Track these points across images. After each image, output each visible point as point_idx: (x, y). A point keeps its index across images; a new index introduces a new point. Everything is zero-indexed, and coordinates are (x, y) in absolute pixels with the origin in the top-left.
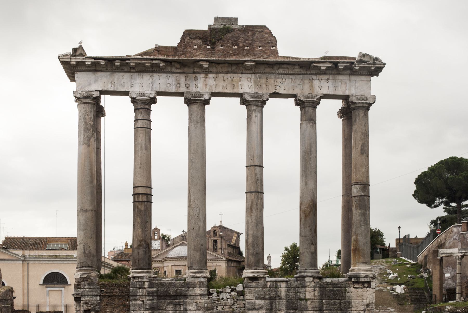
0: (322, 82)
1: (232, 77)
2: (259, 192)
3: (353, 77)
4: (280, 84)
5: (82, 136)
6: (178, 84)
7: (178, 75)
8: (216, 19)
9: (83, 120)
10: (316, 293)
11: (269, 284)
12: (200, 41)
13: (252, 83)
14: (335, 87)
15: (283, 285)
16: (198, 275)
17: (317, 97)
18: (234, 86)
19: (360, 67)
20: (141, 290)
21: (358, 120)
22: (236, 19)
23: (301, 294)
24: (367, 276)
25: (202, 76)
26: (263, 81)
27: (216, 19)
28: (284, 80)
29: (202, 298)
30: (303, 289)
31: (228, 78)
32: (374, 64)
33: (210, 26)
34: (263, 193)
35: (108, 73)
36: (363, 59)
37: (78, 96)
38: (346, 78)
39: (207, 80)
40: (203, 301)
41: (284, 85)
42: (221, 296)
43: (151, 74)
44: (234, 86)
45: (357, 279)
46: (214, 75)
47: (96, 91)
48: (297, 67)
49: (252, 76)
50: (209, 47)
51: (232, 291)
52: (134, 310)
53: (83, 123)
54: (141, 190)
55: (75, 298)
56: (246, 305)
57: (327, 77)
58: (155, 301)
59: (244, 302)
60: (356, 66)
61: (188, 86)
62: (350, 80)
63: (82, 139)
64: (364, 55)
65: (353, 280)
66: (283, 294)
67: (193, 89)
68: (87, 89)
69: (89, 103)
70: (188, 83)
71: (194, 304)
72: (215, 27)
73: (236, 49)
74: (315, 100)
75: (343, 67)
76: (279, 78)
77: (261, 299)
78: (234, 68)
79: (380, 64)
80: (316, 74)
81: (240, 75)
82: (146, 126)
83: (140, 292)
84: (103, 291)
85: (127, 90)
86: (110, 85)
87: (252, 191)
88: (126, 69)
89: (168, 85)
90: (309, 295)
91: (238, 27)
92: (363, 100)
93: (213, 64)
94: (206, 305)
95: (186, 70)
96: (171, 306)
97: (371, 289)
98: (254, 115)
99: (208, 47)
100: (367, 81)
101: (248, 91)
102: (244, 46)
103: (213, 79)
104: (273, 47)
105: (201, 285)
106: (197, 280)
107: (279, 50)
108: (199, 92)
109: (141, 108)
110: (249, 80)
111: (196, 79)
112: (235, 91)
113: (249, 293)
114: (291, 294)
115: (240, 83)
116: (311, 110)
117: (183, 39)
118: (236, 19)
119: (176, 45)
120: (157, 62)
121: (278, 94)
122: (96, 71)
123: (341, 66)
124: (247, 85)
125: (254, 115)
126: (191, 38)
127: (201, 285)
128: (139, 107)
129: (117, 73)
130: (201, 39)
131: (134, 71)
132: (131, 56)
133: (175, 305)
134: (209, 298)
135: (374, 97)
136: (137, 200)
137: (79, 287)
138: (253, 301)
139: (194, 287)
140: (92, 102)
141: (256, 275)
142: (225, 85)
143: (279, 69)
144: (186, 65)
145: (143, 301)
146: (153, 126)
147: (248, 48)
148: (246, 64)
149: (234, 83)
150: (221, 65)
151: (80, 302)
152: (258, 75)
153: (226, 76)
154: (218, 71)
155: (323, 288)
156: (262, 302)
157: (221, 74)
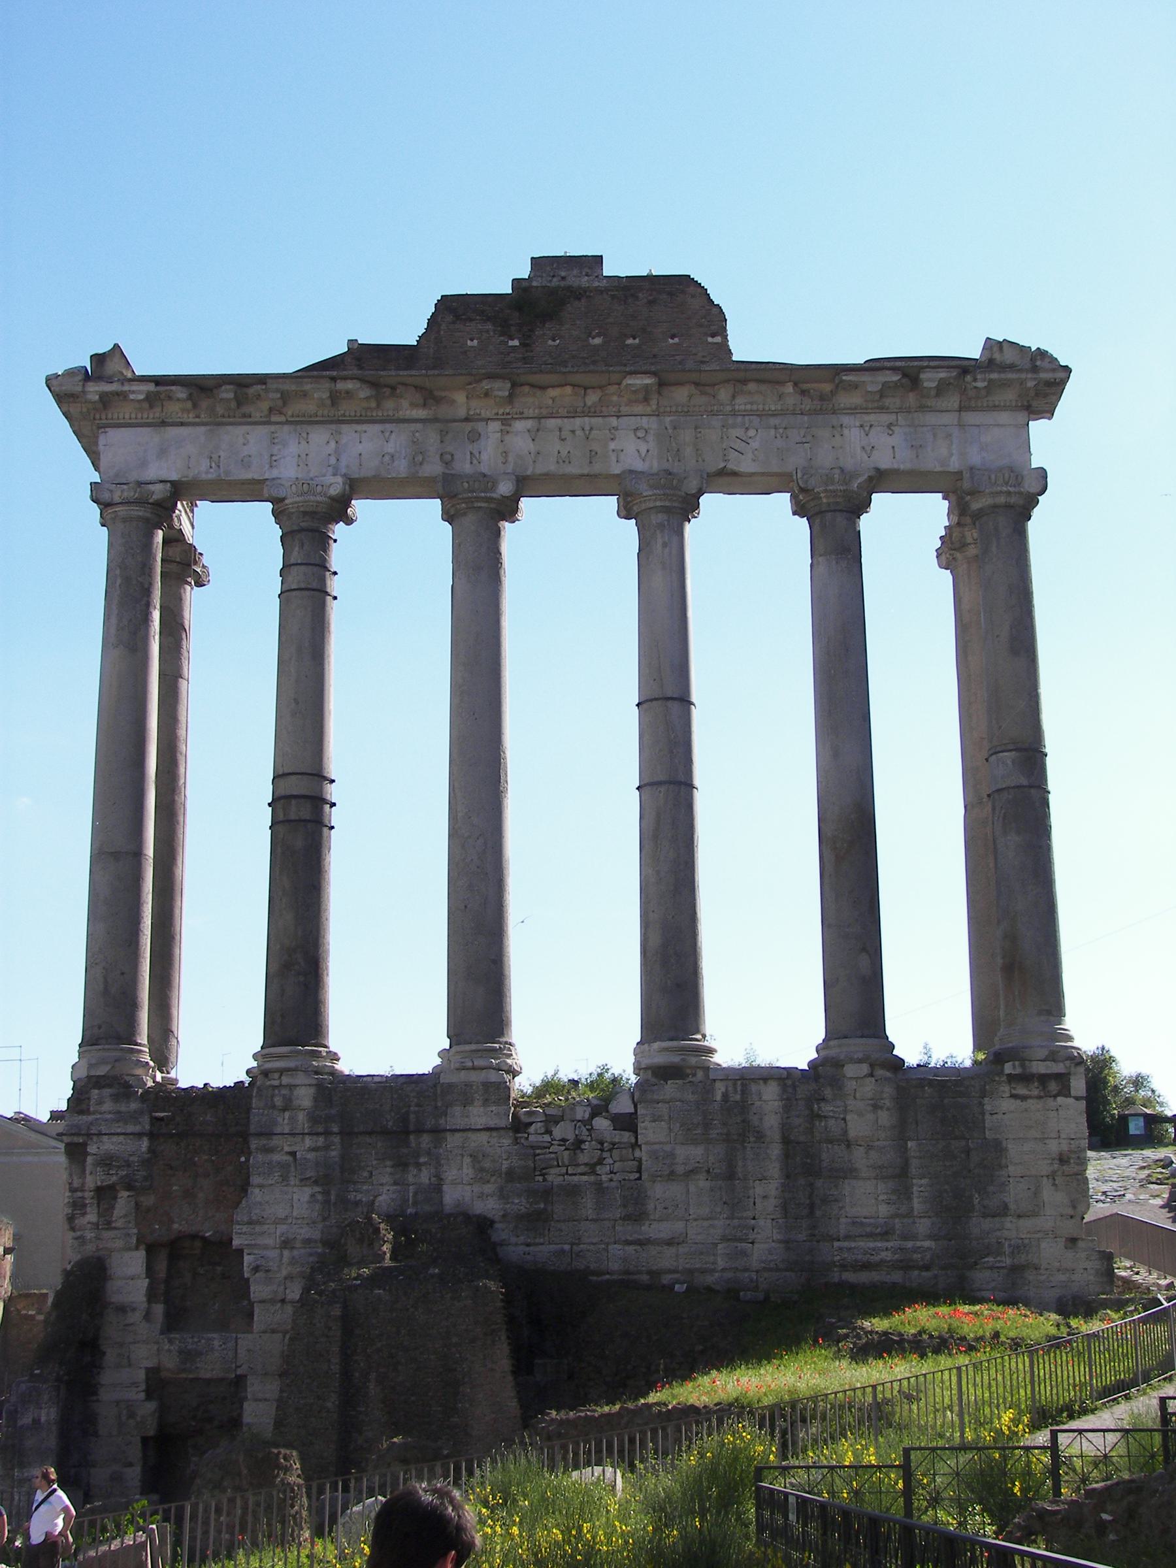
0: (873, 432)
1: (587, 428)
2: (680, 783)
3: (970, 418)
4: (739, 445)
5: (114, 620)
6: (418, 455)
7: (419, 426)
8: (536, 262)
9: (118, 572)
10: (885, 1118)
11: (720, 1088)
12: (489, 326)
13: (652, 444)
14: (917, 448)
15: (771, 1092)
16: (479, 1062)
17: (860, 480)
18: (593, 455)
19: (990, 381)
20: (287, 1114)
21: (994, 549)
22: (599, 260)
23: (832, 1122)
25: (495, 426)
26: (687, 435)
27: (536, 262)
28: (752, 433)
29: (494, 1141)
30: (839, 1103)
31: (573, 432)
32: (1035, 369)
33: (516, 282)
34: (691, 787)
35: (203, 429)
36: (997, 356)
37: (106, 496)
38: (949, 419)
39: (507, 438)
41: (753, 449)
42: (558, 1131)
43: (333, 426)
44: (593, 455)
45: (1023, 1066)
46: (529, 424)
47: (161, 482)
48: (789, 388)
49: (651, 423)
50: (516, 343)
51: (594, 1115)
52: (261, 1186)
53: (119, 581)
54: (295, 786)
55: (68, 1145)
56: (644, 1162)
57: (886, 418)
58: (333, 1153)
59: (637, 1154)
60: (975, 380)
61: (448, 457)
62: (961, 425)
63: (113, 631)
64: (1000, 344)
65: (1008, 1068)
67: (464, 466)
68: (134, 476)
69: (139, 518)
70: (450, 449)
71: (467, 1160)
72: (535, 284)
73: (599, 345)
75: (934, 385)
76: (734, 426)
77: (695, 1142)
78: (592, 398)
79: (1054, 370)
80: (853, 410)
81: (614, 421)
82: (314, 585)
83: (283, 1123)
84: (162, 1119)
85: (256, 477)
86: (204, 464)
87: (656, 779)
88: (257, 416)
89: (387, 458)
90: (858, 1127)
91: (604, 283)
92: (1007, 484)
93: (526, 389)
94: (505, 1165)
95: (444, 411)
96: (389, 1170)
97: (1071, 1101)
98: (660, 541)
99: (511, 343)
100: (1016, 426)
101: (639, 466)
102: (627, 337)
103: (527, 434)
104: (713, 336)
106: (475, 1077)
107: (732, 345)
108: (485, 476)
109: (301, 530)
110: (641, 434)
111: (474, 437)
112: (597, 468)
113: (654, 1121)
114: (797, 1121)
115: (612, 445)
116: (840, 519)
117: (432, 321)
118: (599, 260)
120: (350, 385)
121: (735, 474)
122: (163, 424)
123: (929, 380)
124: (633, 449)
125: (660, 541)
126: (458, 317)
128: (295, 528)
129: (230, 428)
130: (489, 319)
131: (282, 419)
133: (402, 1165)
134: (516, 1141)
135: (1042, 474)
136: (281, 817)
137: (84, 1106)
138: (667, 1148)
139: (467, 1102)
140: (148, 515)
141: (676, 1059)
142: (564, 453)
143: (734, 397)
144: (442, 398)
145: (293, 1154)
146: (335, 585)
147: (637, 341)
148: (629, 382)
149: (595, 447)
150: (552, 392)
151: (85, 1161)
152: (668, 419)
153: (568, 424)
154: (544, 412)
156: (697, 1152)
157: (553, 421)
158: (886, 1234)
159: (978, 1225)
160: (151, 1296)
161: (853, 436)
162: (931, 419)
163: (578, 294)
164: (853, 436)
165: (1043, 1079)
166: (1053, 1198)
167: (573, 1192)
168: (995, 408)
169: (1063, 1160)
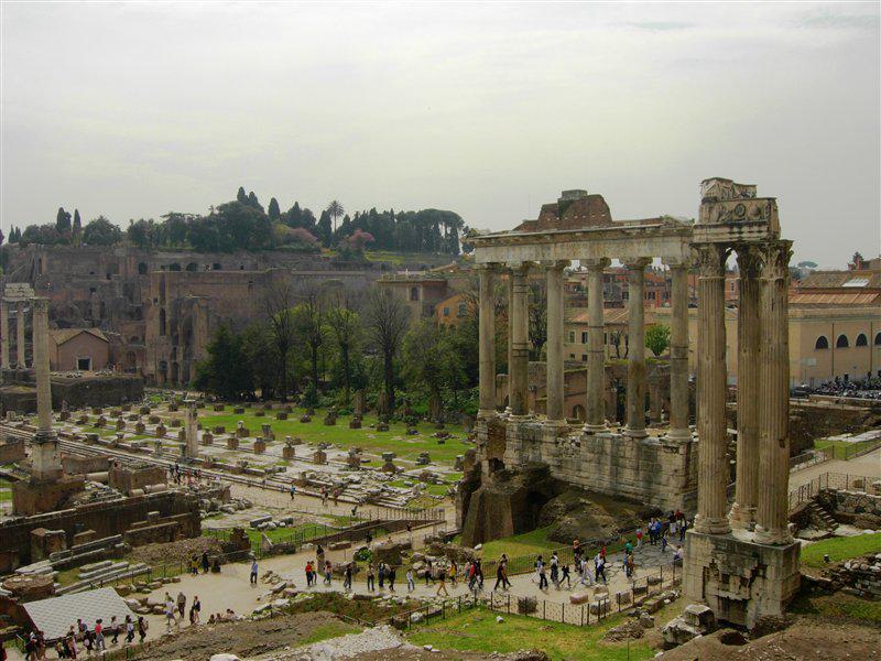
3: (666, 239)
10: (634, 453)
14: (651, 249)
15: (609, 442)
24: (674, 442)
27: (564, 194)
38: (660, 239)
40: (553, 447)
66: (608, 451)
67: (547, 258)
74: (635, 262)
90: (628, 454)
95: (541, 241)
101: (585, 257)
105: (550, 433)
111: (549, 249)
119: (537, 219)
127: (550, 433)
132: (507, 232)
155: (639, 449)
158: (632, 485)
159: (654, 486)
160: (491, 471)
161: (636, 245)
162: (655, 240)
163: (572, 202)
164: (636, 245)
165: (672, 448)
166: (673, 482)
167: (566, 461)
168: (672, 236)
169: (676, 471)
